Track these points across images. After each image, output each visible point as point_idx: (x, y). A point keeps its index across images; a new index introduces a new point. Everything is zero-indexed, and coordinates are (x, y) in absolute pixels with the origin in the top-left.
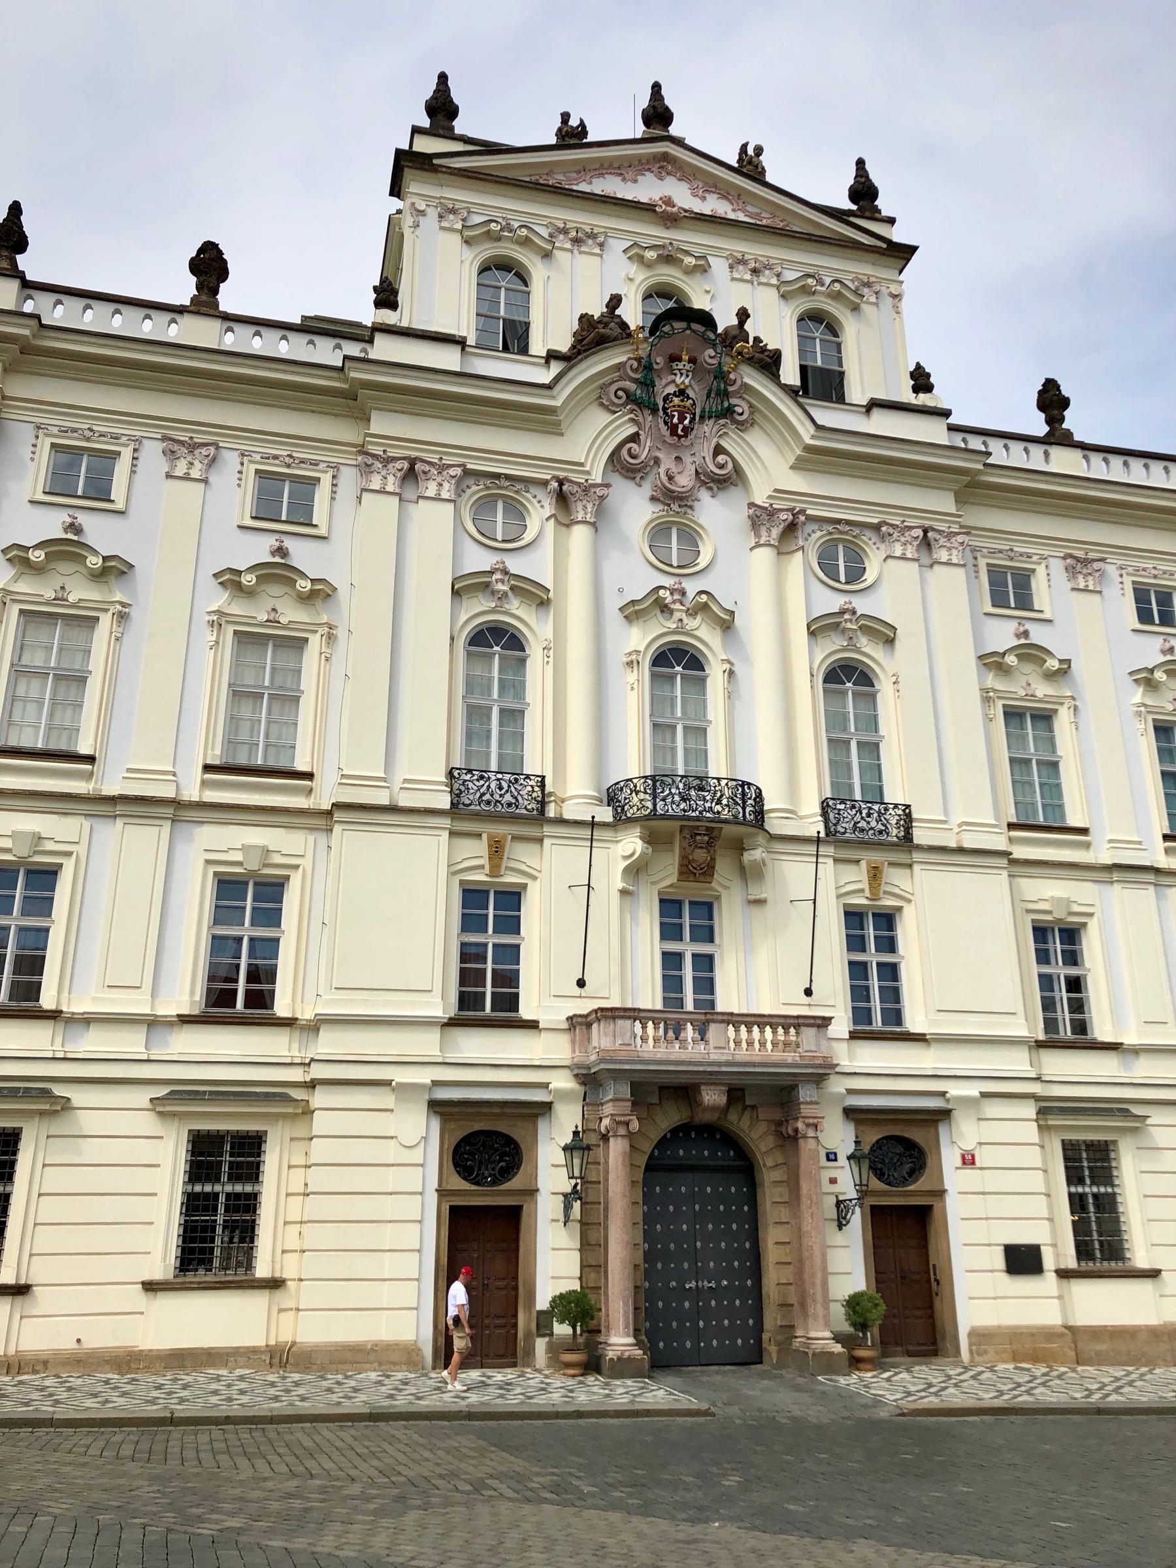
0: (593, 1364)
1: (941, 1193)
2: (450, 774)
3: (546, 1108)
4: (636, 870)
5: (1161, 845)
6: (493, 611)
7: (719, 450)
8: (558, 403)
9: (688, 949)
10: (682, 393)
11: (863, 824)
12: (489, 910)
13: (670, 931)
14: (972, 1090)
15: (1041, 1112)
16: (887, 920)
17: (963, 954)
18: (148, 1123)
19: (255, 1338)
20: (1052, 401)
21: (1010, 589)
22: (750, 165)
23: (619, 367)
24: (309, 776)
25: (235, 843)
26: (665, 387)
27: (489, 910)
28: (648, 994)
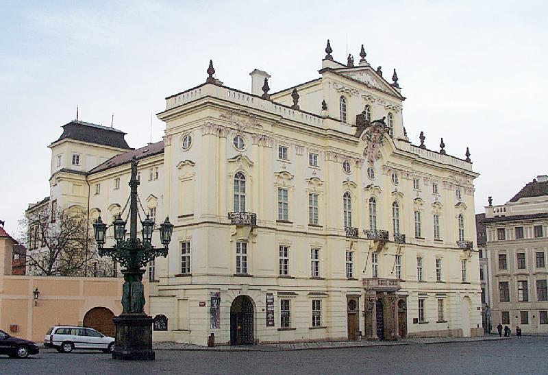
0: (369, 340)
12: (350, 256)
15: (419, 294)
18: (306, 299)
19: (324, 337)
20: (422, 137)
21: (416, 186)
22: (379, 72)
26: (373, 137)
27: (350, 256)
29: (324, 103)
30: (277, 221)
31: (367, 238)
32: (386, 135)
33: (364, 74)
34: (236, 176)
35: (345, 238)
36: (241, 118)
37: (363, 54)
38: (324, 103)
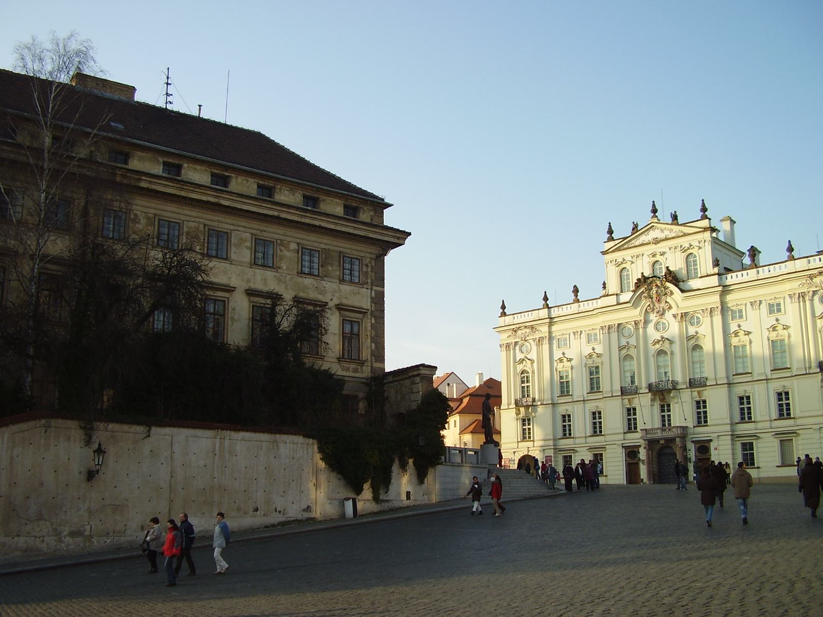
1: (711, 455)
2: (621, 387)
3: (640, 446)
5: (770, 372)
6: (627, 352)
7: (666, 302)
8: (631, 305)
9: (666, 414)
10: (656, 292)
11: (696, 383)
12: (631, 411)
13: (663, 411)
14: (716, 435)
16: (704, 402)
17: (719, 407)
22: (675, 217)
25: (591, 407)
27: (631, 411)
28: (657, 424)
29: (604, 284)
30: (558, 397)
32: (668, 284)
34: (522, 373)
35: (620, 397)
36: (523, 331)
37: (654, 211)
38: (604, 284)
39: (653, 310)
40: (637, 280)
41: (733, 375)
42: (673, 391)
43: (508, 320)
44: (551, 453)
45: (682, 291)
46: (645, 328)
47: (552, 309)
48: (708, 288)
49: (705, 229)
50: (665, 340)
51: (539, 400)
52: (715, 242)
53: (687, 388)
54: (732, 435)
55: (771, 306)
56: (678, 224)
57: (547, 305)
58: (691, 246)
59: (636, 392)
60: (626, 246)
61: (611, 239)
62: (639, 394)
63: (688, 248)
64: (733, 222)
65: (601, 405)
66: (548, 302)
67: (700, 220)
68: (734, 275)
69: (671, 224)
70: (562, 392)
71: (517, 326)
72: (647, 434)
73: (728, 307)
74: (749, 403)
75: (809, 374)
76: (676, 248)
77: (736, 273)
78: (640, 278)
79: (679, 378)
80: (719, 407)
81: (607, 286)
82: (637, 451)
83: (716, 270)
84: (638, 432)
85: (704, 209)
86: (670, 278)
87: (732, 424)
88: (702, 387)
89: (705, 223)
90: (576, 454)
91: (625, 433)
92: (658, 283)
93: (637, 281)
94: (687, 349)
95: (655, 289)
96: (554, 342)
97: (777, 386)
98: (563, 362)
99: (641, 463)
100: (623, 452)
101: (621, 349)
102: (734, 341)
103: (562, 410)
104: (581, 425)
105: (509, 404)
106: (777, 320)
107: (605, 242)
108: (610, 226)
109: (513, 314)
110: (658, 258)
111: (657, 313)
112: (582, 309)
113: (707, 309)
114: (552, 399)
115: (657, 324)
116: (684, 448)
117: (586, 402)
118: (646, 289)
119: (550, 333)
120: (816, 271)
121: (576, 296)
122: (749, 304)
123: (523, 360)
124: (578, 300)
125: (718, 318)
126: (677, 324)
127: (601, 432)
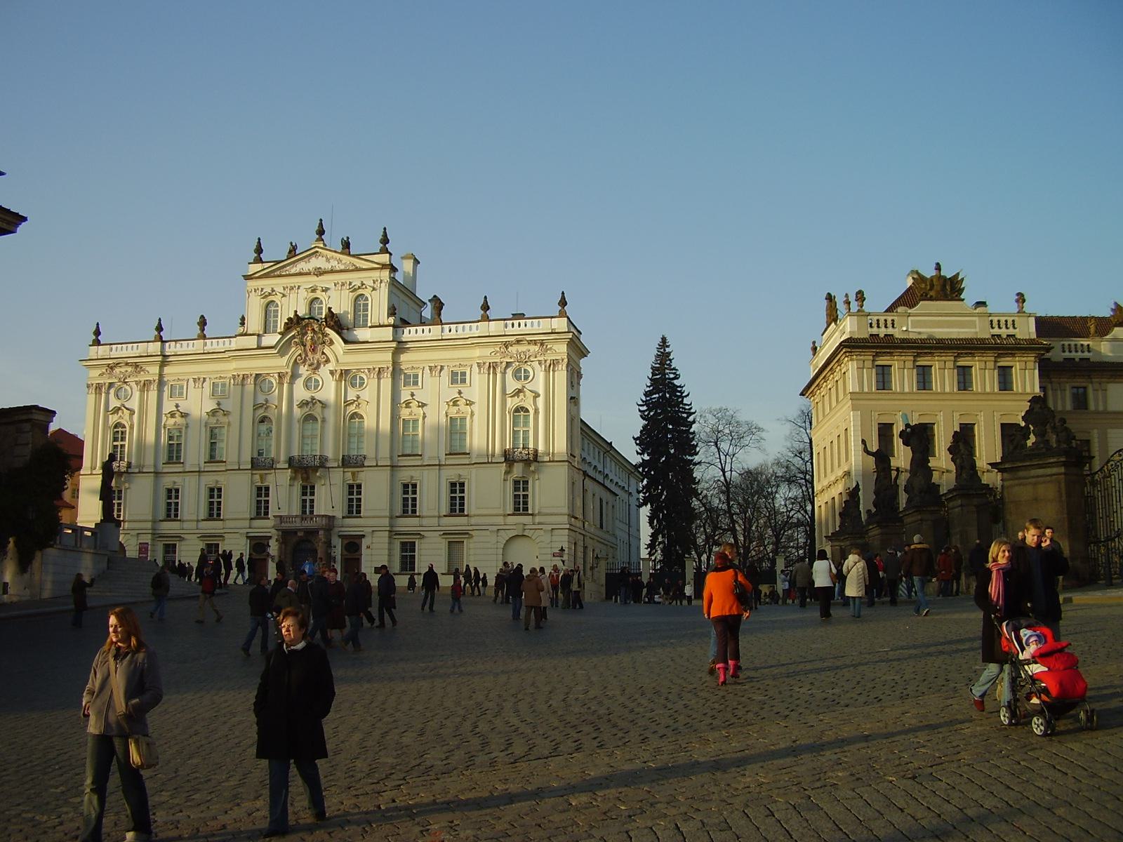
2: (252, 458)
3: (271, 537)
4: (293, 479)
7: (323, 353)
8: (276, 352)
9: (308, 498)
12: (262, 491)
13: (304, 494)
16: (359, 486)
17: (377, 493)
22: (346, 245)
23: (293, 335)
24: (225, 462)
25: (209, 480)
27: (262, 491)
28: (296, 510)
31: (287, 467)
32: (328, 330)
33: (313, 259)
36: (123, 370)
37: (321, 232)
38: (243, 319)
39: (304, 362)
40: (288, 319)
41: (399, 456)
42: (321, 469)
43: (102, 351)
44: (147, 539)
45: (346, 342)
46: (291, 383)
47: (167, 344)
48: (379, 342)
49: (384, 266)
50: (316, 403)
51: (137, 467)
52: (393, 284)
53: (338, 467)
54: (390, 531)
55: (454, 374)
56: (349, 254)
57: (161, 337)
58: (363, 284)
59: (271, 466)
60: (278, 273)
61: (259, 260)
62: (275, 469)
63: (359, 288)
64: (417, 262)
65: (222, 480)
66: (162, 333)
67: (378, 253)
68: (412, 329)
69: (341, 253)
70: (170, 458)
71: (115, 361)
72: (281, 523)
73: (401, 369)
74: (414, 492)
75: (492, 463)
76: (343, 284)
77: (415, 328)
78: (292, 317)
79: (329, 453)
80: (377, 493)
81: (246, 322)
82: (266, 543)
83: (391, 320)
84: (269, 519)
85: (385, 240)
86: (332, 323)
87: (391, 518)
88: (358, 467)
89: (384, 258)
90: (183, 543)
91: (251, 519)
92: (316, 327)
93: (286, 321)
94: (344, 416)
95: (310, 334)
96: (166, 388)
97: (451, 474)
98: (175, 417)
99: (270, 560)
100: (246, 544)
101: (256, 407)
102: (405, 413)
103: (167, 482)
104: (192, 504)
105: (93, 468)
106: (460, 393)
107: (250, 263)
108: (259, 242)
109: (111, 344)
110: (318, 294)
111: (309, 365)
112: (209, 348)
113: (374, 369)
114: (155, 466)
115: (308, 380)
116: (329, 544)
117: (202, 474)
118: (298, 332)
119: (161, 375)
120: (513, 339)
121: (203, 330)
122: (427, 369)
123: (119, 409)
124: (205, 336)
125: (387, 383)
126: (333, 384)
127: (219, 515)
